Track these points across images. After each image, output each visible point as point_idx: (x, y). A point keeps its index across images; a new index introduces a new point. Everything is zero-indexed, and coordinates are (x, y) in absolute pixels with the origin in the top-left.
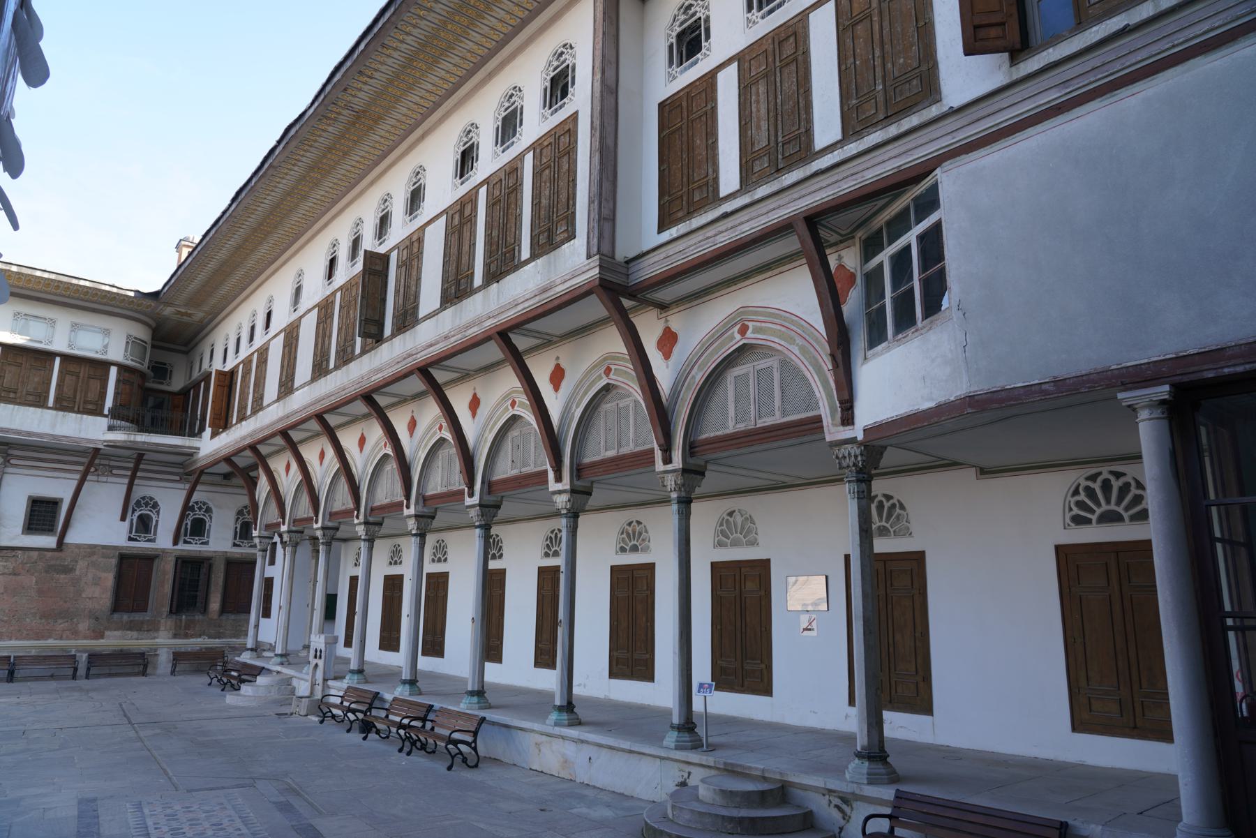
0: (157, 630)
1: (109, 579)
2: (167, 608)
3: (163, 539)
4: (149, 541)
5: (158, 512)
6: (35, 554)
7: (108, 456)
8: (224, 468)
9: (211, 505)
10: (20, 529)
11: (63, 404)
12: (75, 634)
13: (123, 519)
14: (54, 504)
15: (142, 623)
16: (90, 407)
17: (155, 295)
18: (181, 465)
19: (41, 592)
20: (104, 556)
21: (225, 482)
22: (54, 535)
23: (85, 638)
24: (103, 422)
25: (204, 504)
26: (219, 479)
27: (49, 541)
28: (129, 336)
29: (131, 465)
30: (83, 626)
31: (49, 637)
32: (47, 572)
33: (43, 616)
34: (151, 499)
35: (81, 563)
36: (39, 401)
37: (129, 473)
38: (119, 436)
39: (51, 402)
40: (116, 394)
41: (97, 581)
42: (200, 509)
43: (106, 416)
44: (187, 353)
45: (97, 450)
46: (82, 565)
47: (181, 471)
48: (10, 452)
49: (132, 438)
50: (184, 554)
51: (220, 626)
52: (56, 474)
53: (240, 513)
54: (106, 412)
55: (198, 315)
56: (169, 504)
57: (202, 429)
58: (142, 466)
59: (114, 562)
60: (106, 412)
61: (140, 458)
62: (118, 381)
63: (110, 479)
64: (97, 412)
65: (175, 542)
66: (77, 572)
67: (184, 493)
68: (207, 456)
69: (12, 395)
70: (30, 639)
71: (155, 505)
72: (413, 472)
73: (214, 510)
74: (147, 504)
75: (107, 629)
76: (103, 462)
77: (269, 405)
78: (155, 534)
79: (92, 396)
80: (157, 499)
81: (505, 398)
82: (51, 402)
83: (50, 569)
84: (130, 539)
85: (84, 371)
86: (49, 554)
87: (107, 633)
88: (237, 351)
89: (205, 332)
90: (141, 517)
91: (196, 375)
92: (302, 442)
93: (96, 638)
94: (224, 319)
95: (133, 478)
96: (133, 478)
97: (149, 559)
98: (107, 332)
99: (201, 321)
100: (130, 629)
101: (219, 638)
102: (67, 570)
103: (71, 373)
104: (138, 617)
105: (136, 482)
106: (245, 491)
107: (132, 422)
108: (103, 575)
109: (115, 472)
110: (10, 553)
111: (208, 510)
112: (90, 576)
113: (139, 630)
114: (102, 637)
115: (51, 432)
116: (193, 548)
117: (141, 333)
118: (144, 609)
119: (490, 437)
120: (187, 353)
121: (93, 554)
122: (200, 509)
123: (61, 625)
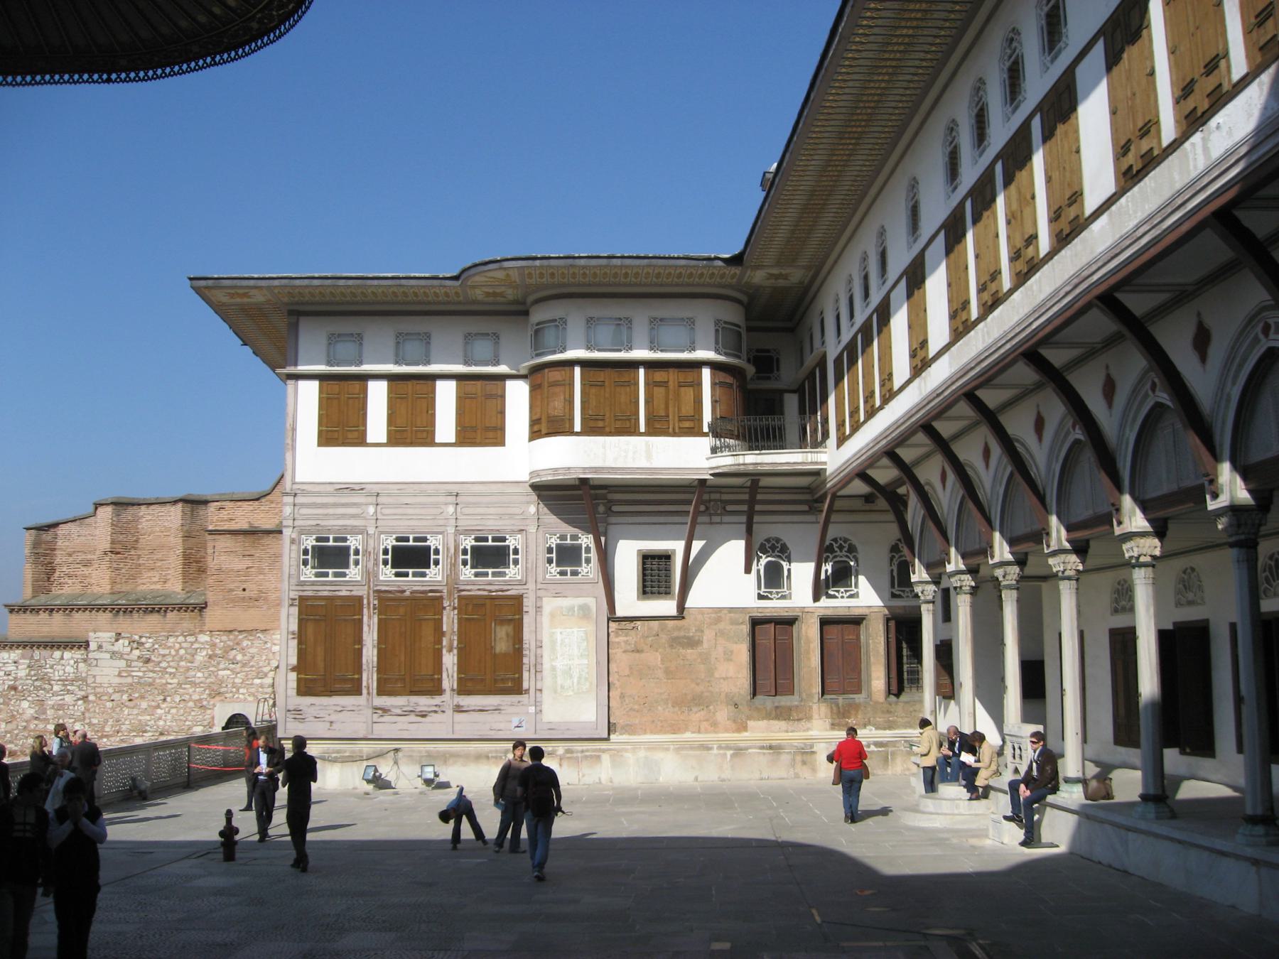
0: (809, 718)
1: (742, 652)
2: (817, 689)
4: (783, 597)
7: (718, 489)
8: (859, 487)
9: (855, 542)
11: (656, 428)
12: (715, 726)
13: (748, 570)
14: (667, 557)
15: (790, 709)
16: (687, 424)
17: (736, 260)
18: (808, 489)
19: (668, 673)
20: (733, 622)
21: (868, 507)
22: (673, 599)
23: (727, 730)
24: (706, 443)
25: (846, 540)
26: (859, 504)
27: (667, 607)
28: (717, 322)
29: (746, 497)
30: (723, 714)
31: (686, 730)
32: (671, 646)
33: (676, 703)
34: (778, 540)
35: (707, 632)
36: (628, 429)
37: (745, 508)
38: (726, 461)
39: (642, 429)
40: (714, 402)
41: (728, 655)
42: (841, 548)
43: (706, 435)
44: (792, 330)
45: (702, 482)
46: (708, 635)
48: (610, 496)
49: (741, 460)
50: (829, 613)
51: (889, 712)
52: (662, 519)
54: (706, 429)
55: (796, 275)
57: (826, 435)
58: (759, 497)
60: (706, 429)
62: (713, 384)
63: (726, 519)
64: (695, 431)
65: (816, 598)
66: (705, 645)
67: (819, 527)
68: (839, 471)
69: (600, 424)
70: (665, 733)
72: (1120, 465)
73: (859, 548)
74: (773, 548)
75: (750, 718)
76: (714, 496)
77: (902, 389)
78: (789, 588)
79: (687, 409)
80: (785, 539)
81: (1251, 320)
82: (642, 429)
83: (676, 642)
84: (761, 597)
85: (672, 376)
86: (670, 623)
87: (751, 723)
88: (852, 316)
89: (811, 294)
90: (768, 565)
91: (810, 361)
92: (957, 436)
93: (738, 730)
94: (829, 272)
95: (750, 515)
96: (750, 515)
97: (787, 623)
98: (691, 322)
99: (801, 283)
100: (777, 718)
101: (890, 728)
102: (693, 643)
103: (658, 384)
104: (784, 701)
105: (756, 518)
106: (891, 517)
107: (737, 438)
108: (735, 647)
109: (729, 508)
110: (629, 625)
111: (852, 549)
112: (720, 649)
113: (787, 718)
114: (745, 728)
115: (648, 465)
116: (837, 603)
117: (732, 314)
118: (790, 691)
119: (1235, 392)
120: (792, 330)
121: (718, 620)
122: (841, 548)
123: (697, 715)
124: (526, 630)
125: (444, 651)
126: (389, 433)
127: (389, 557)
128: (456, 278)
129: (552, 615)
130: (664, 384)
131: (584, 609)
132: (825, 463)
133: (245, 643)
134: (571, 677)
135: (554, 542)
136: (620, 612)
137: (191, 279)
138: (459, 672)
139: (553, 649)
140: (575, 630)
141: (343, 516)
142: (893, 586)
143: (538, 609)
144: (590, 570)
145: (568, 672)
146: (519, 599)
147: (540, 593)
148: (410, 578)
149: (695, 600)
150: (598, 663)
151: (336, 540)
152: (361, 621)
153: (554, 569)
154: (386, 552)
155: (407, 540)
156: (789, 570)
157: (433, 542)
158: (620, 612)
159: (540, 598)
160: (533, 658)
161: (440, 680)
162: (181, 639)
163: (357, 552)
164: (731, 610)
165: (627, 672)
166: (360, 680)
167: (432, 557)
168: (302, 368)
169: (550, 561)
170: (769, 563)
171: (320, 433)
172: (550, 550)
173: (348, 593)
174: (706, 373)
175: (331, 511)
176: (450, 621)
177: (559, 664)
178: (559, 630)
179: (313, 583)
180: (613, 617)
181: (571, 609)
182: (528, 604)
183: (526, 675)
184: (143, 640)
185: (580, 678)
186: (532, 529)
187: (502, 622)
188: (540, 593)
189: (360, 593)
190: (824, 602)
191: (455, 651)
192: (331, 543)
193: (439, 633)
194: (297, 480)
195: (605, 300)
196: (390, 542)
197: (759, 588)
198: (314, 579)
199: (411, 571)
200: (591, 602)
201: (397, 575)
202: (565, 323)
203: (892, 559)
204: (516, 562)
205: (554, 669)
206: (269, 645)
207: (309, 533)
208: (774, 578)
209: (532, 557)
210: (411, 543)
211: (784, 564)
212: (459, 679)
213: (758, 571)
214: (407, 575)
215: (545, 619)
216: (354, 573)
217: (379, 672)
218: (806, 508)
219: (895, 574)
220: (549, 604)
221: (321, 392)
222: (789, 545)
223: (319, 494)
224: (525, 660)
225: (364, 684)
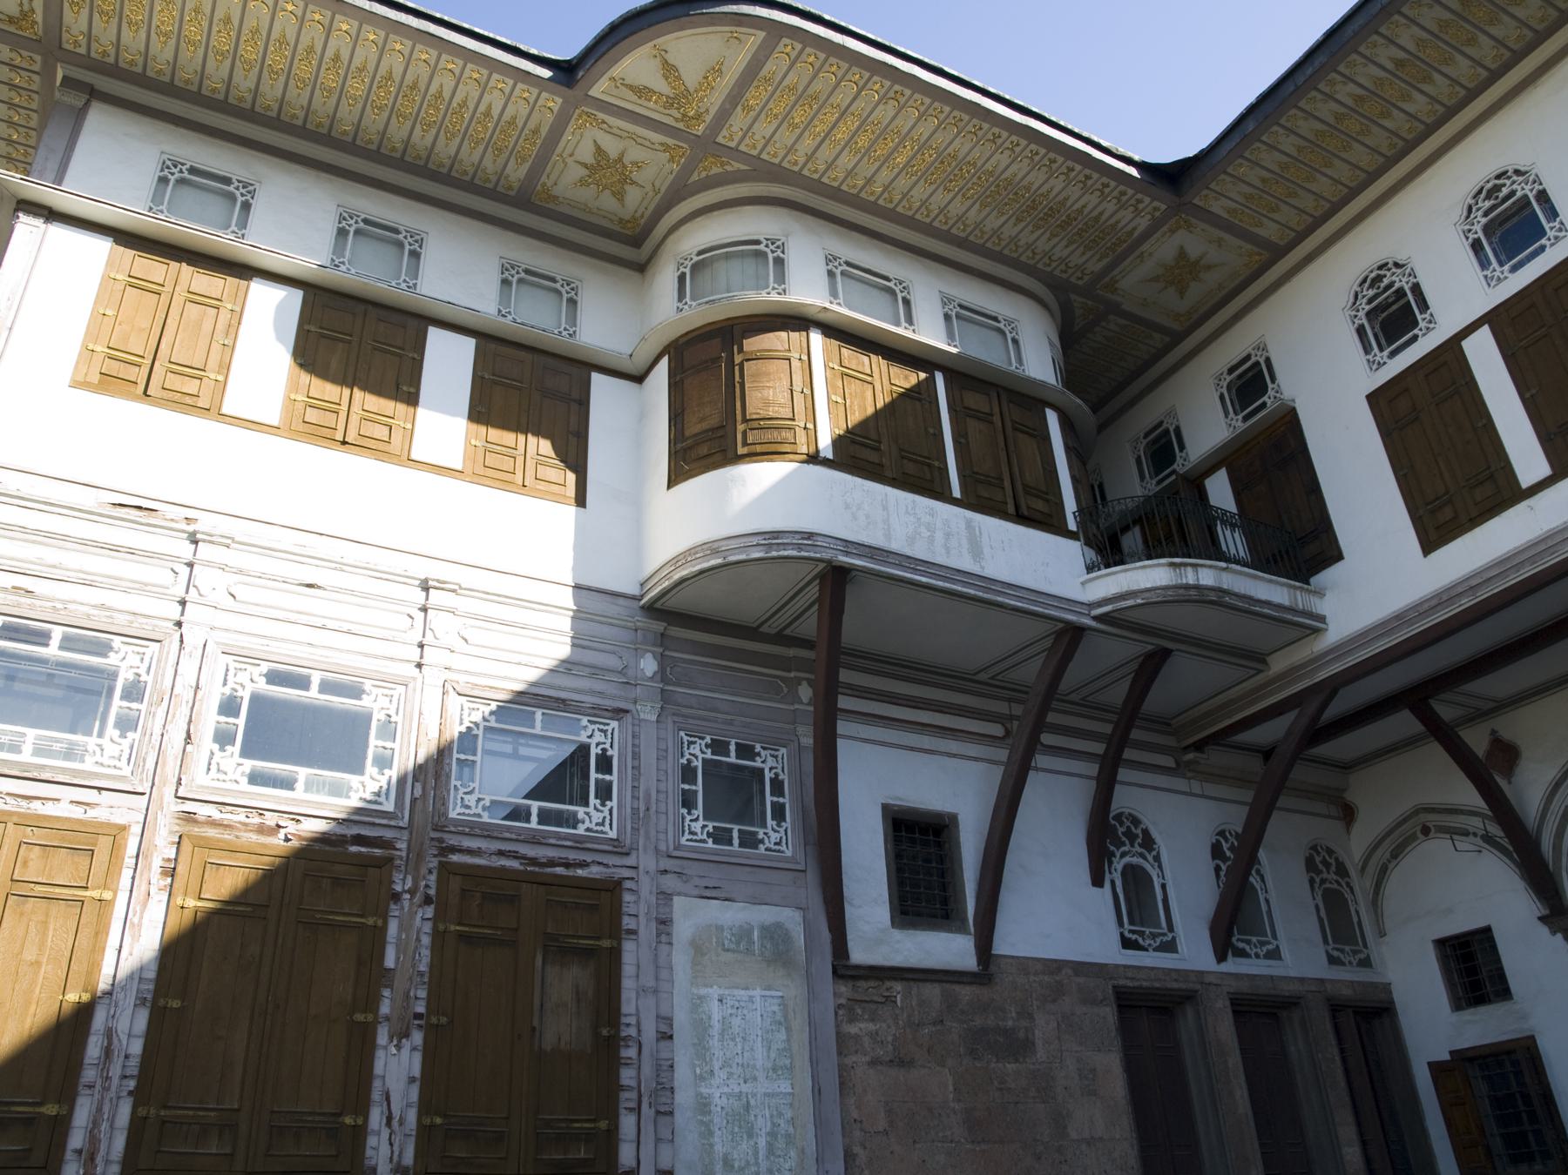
3: (1194, 952)
5: (1157, 858)
6: (932, 991)
10: (881, 912)
13: (1097, 881)
22: (962, 929)
27: (948, 949)
34: (1136, 821)
46: (1043, 1028)
47: (1170, 741)
49: (1190, 577)
52: (926, 741)
53: (1310, 865)
56: (1183, 831)
59: (1109, 1014)
61: (1151, 665)
65: (1221, 958)
66: (1041, 1054)
71: (1148, 842)
74: (1131, 837)
78: (1171, 928)
80: (1147, 822)
84: (1127, 944)
86: (965, 993)
115: (975, 569)
124: (628, 984)
125: (382, 1037)
126: (290, 402)
127: (241, 721)
128: (566, 72)
129: (698, 948)
130: (986, 418)
131: (775, 934)
132: (1322, 619)
134: (750, 1135)
135: (698, 753)
136: (859, 955)
138: (425, 1107)
139: (701, 1049)
140: (757, 992)
141: (114, 583)
142: (1326, 941)
143: (664, 923)
144: (780, 838)
145: (741, 1118)
146: (613, 888)
147: (670, 882)
148: (299, 792)
149: (1012, 940)
150: (817, 1091)
151: (68, 643)
152: (105, 906)
153: (699, 824)
154: (229, 707)
155: (302, 683)
156: (1164, 886)
157: (375, 703)
158: (859, 955)
159: (665, 897)
160: (647, 1070)
161: (359, 1133)
163: (134, 692)
164: (1080, 968)
165: (882, 1124)
166: (62, 1125)
167: (374, 742)
169: (688, 801)
170: (1125, 867)
172: (688, 773)
173: (77, 813)
174: (1052, 419)
176: (408, 936)
177: (719, 1091)
178: (714, 992)
180: (844, 970)
181: (744, 933)
182: (637, 908)
183: (627, 1123)
185: (772, 1134)
186: (648, 713)
187: (560, 950)
188: (670, 882)
189: (118, 819)
190: (1232, 965)
191: (418, 1037)
192: (52, 651)
193: (370, 973)
195: (864, 238)
196: (251, 683)
197: (1120, 923)
199: (302, 773)
200: (790, 918)
201: (255, 778)
202: (782, 248)
203: (1312, 881)
204: (605, 792)
205: (704, 1106)
208: (1139, 905)
209: (649, 781)
210: (313, 694)
211: (1154, 873)
212: (425, 1134)
213: (1113, 883)
214: (288, 784)
215: (680, 959)
216: (103, 751)
217: (140, 1096)
218: (1168, 761)
219: (1323, 913)
220: (692, 916)
221: (110, 263)
222: (1155, 834)
224: (627, 1076)
225: (76, 1140)
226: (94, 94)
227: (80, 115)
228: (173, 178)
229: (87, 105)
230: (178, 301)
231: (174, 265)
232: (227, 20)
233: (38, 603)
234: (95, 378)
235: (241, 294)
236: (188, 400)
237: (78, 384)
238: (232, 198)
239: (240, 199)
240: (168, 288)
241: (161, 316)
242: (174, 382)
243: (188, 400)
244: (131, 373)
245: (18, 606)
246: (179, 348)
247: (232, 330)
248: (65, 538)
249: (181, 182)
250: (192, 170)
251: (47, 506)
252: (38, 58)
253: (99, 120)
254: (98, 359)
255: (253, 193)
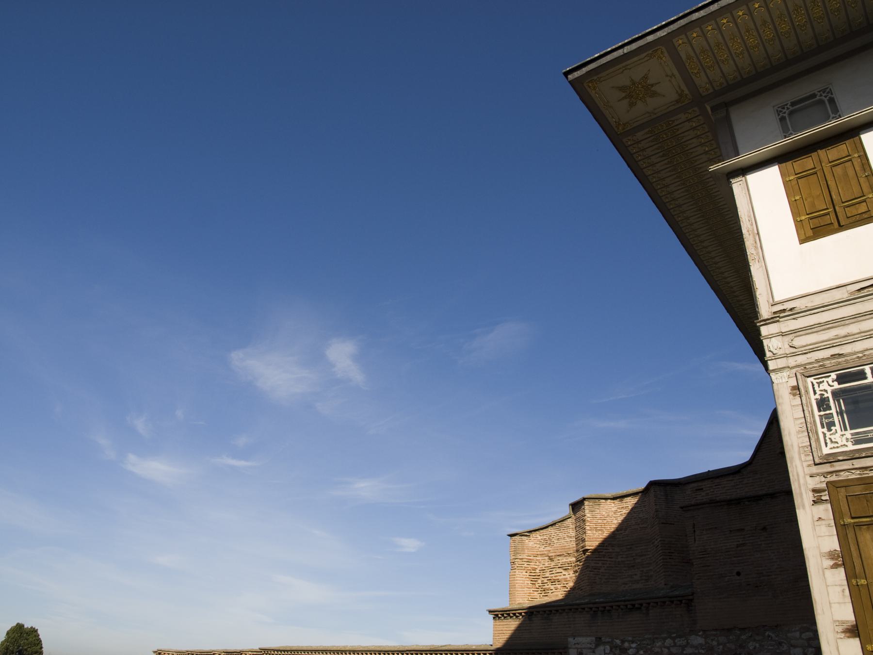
133: (751, 645)
137: (566, 74)
162: (668, 642)
168: (746, 157)
171: (799, 224)
175: (854, 328)
179: (852, 456)
184: (626, 645)
194: (777, 299)
198: (851, 447)
206: (785, 647)
207: (821, 373)
223: (825, 307)
226: (727, 105)
227: (727, 119)
228: (786, 115)
229: (727, 111)
230: (827, 170)
231: (814, 155)
232: (764, 22)
233: (848, 358)
234: (810, 233)
235: (858, 145)
236: (865, 216)
237: (802, 241)
238: (821, 102)
239: (826, 100)
240: (819, 168)
241: (823, 183)
242: (851, 211)
243: (865, 216)
244: (827, 220)
245: (839, 363)
246: (843, 192)
247: (866, 166)
248: (843, 319)
249: (791, 113)
250: (793, 104)
251: (825, 307)
252: (696, 109)
253: (736, 115)
254: (806, 224)
255: (831, 92)
